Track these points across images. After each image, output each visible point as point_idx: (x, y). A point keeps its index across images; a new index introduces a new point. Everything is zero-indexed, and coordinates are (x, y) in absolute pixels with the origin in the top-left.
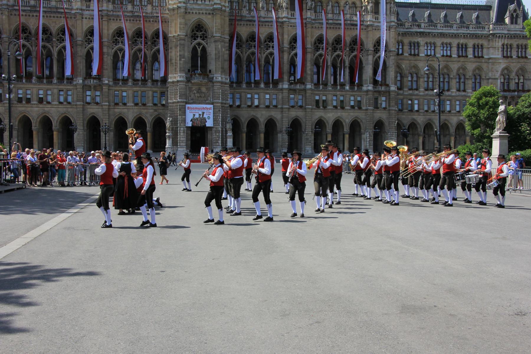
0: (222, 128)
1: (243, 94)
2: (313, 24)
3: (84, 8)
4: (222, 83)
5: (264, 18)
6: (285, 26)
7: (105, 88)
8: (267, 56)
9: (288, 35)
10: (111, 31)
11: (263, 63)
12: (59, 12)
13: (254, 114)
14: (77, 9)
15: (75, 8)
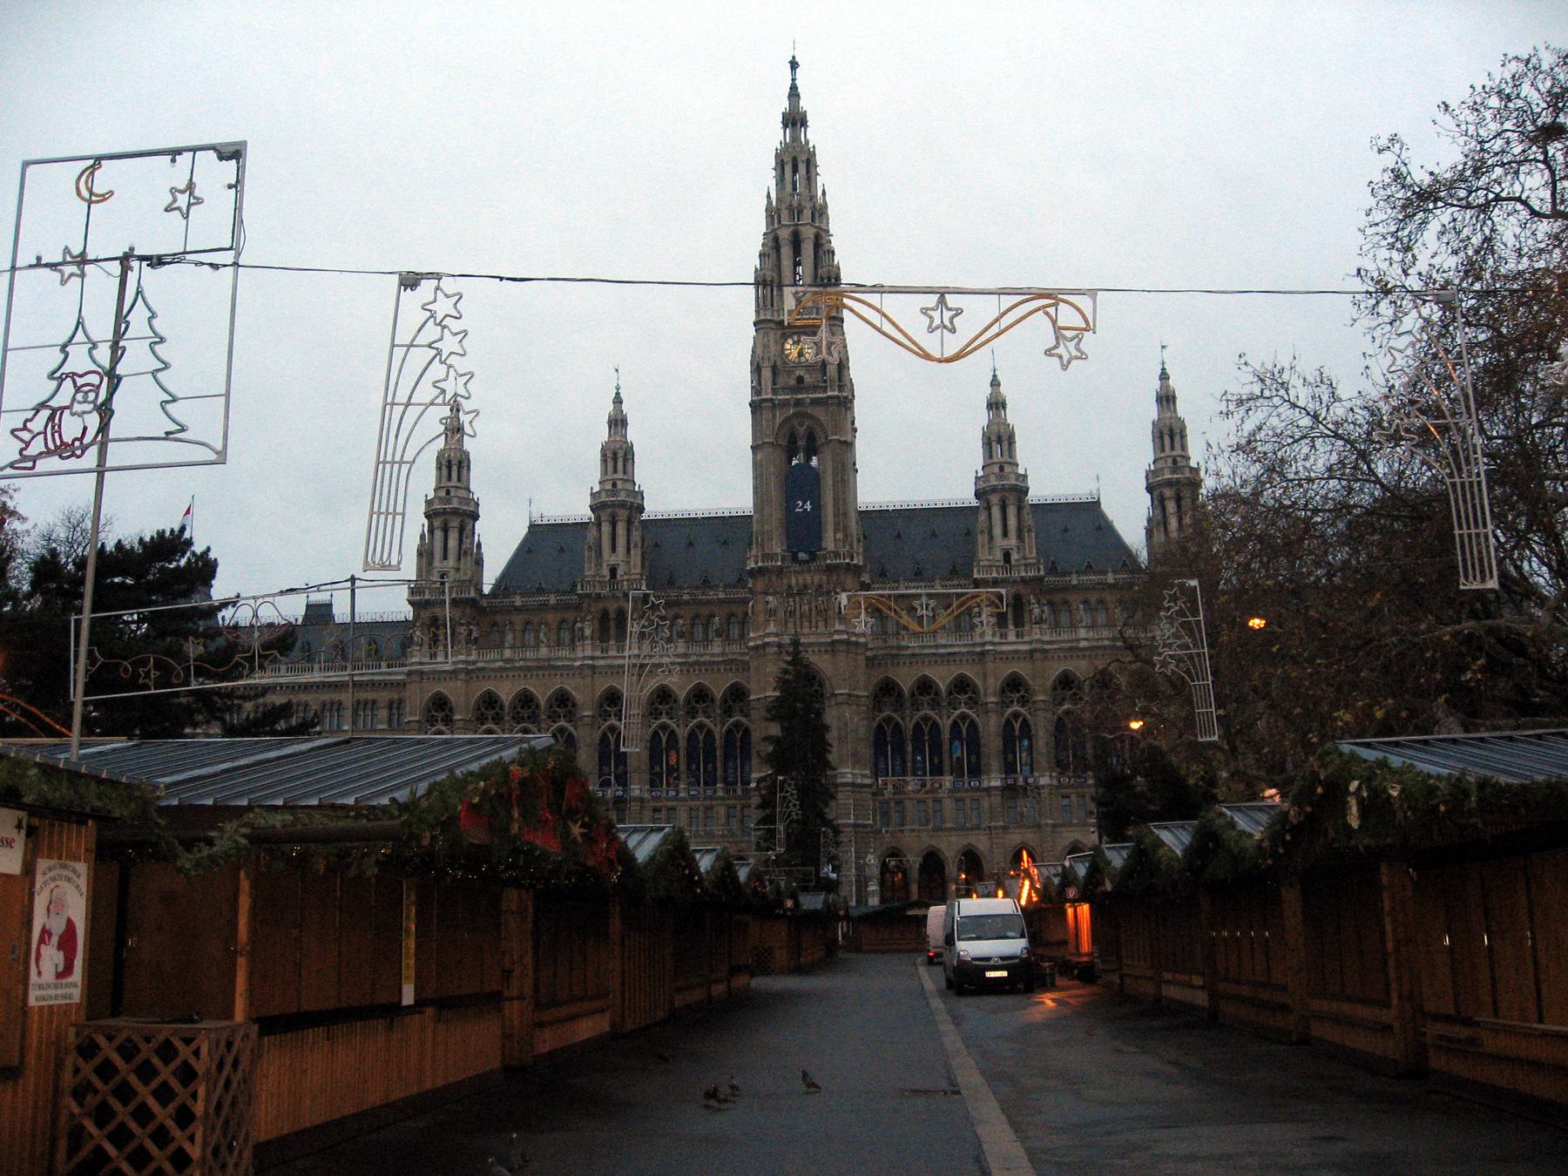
0: (858, 876)
1: (908, 803)
2: (1046, 651)
3: (598, 653)
4: (853, 785)
5: (945, 646)
6: (989, 658)
7: (635, 806)
8: (955, 722)
9: (996, 678)
10: (646, 692)
11: (946, 735)
12: (553, 667)
13: (934, 843)
14: (584, 658)
15: (580, 655)
